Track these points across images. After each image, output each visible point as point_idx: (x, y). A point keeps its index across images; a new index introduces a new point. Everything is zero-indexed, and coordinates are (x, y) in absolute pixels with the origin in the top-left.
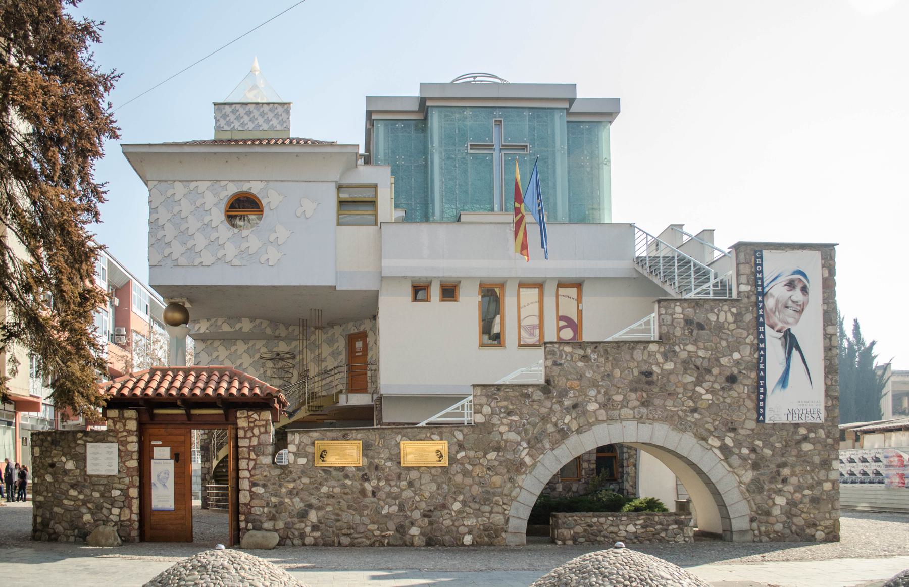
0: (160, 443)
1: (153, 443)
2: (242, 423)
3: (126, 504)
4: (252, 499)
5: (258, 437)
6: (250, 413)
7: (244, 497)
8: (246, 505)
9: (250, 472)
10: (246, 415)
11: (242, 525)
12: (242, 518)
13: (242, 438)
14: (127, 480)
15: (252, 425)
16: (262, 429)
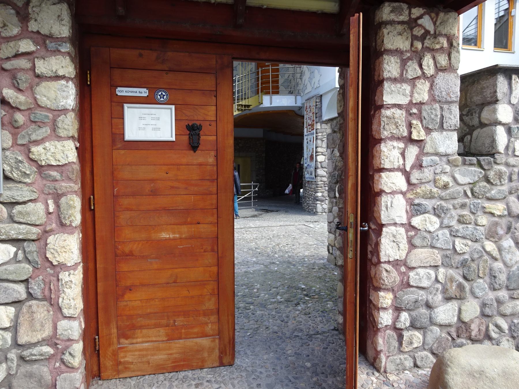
0: (144, 92)
1: (122, 92)
2: (394, 40)
3: (36, 288)
4: (412, 246)
5: (431, 79)
6: (416, 12)
7: (391, 246)
8: (396, 264)
9: (407, 175)
10: (404, 17)
11: (385, 318)
12: (385, 299)
13: (395, 80)
14: (37, 211)
15: (419, 45)
16: (443, 60)
